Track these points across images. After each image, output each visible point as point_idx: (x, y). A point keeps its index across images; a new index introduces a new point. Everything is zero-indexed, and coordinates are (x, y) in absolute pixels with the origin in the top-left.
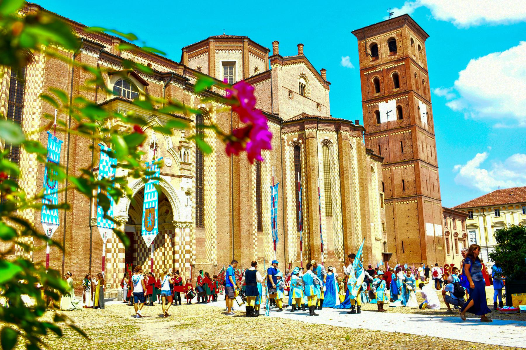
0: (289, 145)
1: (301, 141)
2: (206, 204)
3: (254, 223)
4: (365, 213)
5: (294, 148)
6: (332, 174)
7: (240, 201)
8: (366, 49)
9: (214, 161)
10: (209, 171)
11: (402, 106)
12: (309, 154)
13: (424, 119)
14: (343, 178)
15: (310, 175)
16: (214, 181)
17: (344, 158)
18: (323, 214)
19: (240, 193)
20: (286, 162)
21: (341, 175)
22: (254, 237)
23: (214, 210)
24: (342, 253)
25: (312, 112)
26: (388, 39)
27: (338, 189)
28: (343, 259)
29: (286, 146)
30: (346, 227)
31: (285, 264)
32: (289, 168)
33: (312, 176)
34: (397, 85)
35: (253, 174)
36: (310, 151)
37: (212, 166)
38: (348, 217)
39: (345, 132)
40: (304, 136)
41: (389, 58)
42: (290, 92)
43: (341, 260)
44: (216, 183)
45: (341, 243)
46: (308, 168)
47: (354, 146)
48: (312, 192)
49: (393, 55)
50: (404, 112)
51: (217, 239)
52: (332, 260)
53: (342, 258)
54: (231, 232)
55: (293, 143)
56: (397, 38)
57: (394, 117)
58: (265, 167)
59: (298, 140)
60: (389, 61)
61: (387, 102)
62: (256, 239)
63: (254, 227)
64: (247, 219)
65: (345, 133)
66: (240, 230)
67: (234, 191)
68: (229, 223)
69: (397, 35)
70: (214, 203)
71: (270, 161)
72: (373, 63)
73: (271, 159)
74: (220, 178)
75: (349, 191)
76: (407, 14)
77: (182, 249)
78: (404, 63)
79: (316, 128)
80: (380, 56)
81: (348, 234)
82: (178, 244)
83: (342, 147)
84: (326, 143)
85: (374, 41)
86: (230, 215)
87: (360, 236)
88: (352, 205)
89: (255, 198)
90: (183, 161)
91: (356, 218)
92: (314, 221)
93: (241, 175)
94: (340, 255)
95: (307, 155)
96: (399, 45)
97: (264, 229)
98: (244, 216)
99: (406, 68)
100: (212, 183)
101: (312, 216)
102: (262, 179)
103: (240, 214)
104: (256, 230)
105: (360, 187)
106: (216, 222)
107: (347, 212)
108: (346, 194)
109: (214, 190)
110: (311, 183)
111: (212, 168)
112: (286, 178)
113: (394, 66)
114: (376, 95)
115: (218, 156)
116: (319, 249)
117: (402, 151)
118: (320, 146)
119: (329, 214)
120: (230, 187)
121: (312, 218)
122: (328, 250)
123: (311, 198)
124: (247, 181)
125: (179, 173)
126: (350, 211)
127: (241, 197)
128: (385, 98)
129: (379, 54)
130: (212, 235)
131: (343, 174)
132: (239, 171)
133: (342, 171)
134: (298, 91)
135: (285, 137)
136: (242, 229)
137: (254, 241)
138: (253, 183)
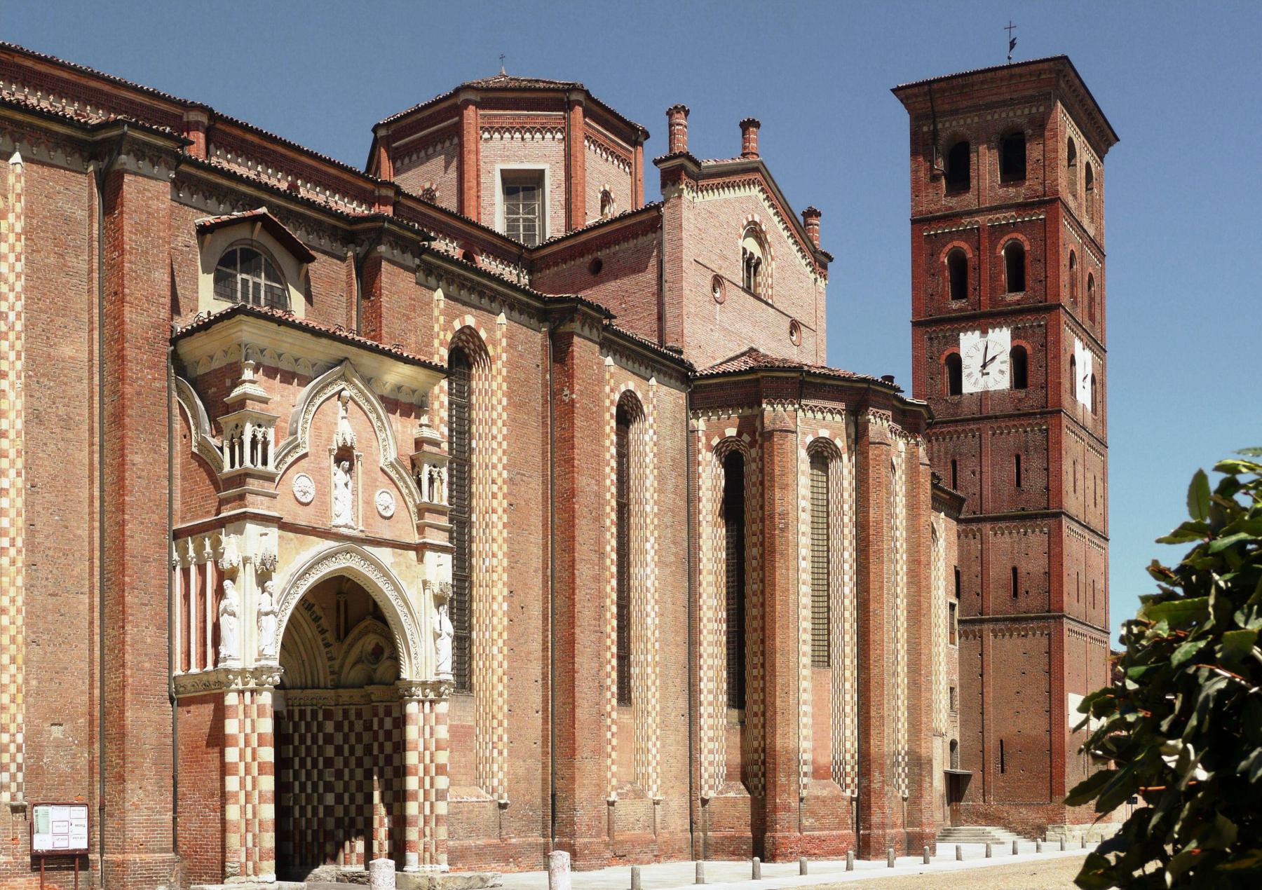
0: (709, 448)
2: (476, 627)
3: (609, 681)
4: (920, 659)
5: (726, 457)
6: (835, 542)
7: (574, 617)
9: (500, 495)
10: (487, 525)
12: (772, 480)
14: (867, 558)
15: (773, 544)
16: (500, 555)
17: (873, 497)
18: (806, 660)
19: (574, 594)
22: (609, 721)
23: (500, 643)
24: (853, 774)
25: (778, 348)
27: (849, 589)
29: (704, 451)
30: (869, 701)
31: (691, 801)
33: (779, 548)
35: (608, 535)
36: (777, 472)
37: (494, 511)
38: (874, 671)
39: (878, 420)
40: (758, 423)
43: (848, 792)
44: (505, 562)
45: (851, 744)
46: (767, 522)
47: (899, 461)
48: (778, 593)
51: (509, 731)
52: (825, 793)
53: (852, 786)
54: (545, 710)
58: (644, 514)
59: (739, 434)
62: (614, 728)
63: (609, 695)
64: (593, 672)
65: (879, 424)
66: (573, 703)
67: (557, 586)
68: (540, 682)
70: (500, 621)
71: (656, 495)
73: (660, 491)
74: (516, 547)
75: (881, 595)
81: (873, 721)
83: (868, 465)
84: (821, 455)
86: (545, 658)
87: (903, 725)
88: (889, 638)
89: (614, 609)
90: (426, 499)
91: (895, 674)
92: (779, 681)
93: (579, 539)
94: (848, 780)
95: (767, 484)
97: (634, 700)
98: (584, 663)
100: (495, 561)
101: (774, 666)
102: (633, 551)
103: (573, 657)
104: (614, 702)
105: (908, 583)
106: (505, 679)
107: (872, 658)
108: (873, 606)
109: (500, 585)
110: (774, 567)
111: (495, 517)
115: (511, 479)
116: (789, 760)
118: (803, 454)
119: (823, 658)
120: (545, 575)
121: (774, 670)
122: (814, 762)
123: (774, 612)
124: (594, 557)
125: (415, 539)
126: (881, 656)
127: (578, 607)
130: (493, 717)
131: (868, 546)
132: (573, 526)
133: (864, 534)
135: (701, 424)
136: (579, 702)
137: (609, 735)
138: (608, 562)
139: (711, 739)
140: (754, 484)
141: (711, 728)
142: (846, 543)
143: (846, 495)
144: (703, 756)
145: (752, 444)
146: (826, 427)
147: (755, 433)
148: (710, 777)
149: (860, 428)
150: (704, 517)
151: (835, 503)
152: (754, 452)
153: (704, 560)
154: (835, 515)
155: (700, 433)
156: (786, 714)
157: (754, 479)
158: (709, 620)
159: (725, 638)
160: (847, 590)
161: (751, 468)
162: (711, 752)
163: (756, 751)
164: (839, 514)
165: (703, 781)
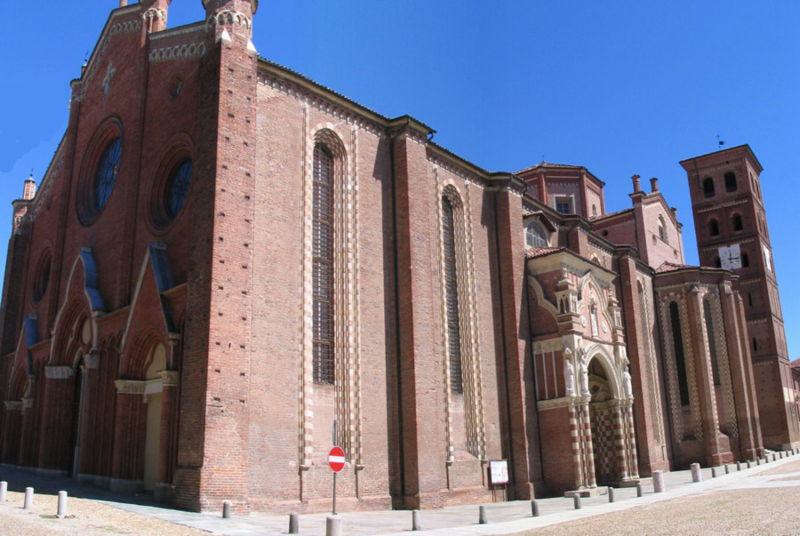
11: (748, 252)
13: (769, 267)
34: (739, 227)
41: (728, 194)
42: (654, 237)
50: (750, 258)
57: (738, 265)
61: (729, 246)
72: (708, 200)
76: (747, 145)
96: (738, 180)
99: (750, 207)
114: (714, 238)
117: (751, 304)
128: (728, 242)
134: (658, 234)
145: (682, 298)
152: (682, 301)
161: (682, 308)
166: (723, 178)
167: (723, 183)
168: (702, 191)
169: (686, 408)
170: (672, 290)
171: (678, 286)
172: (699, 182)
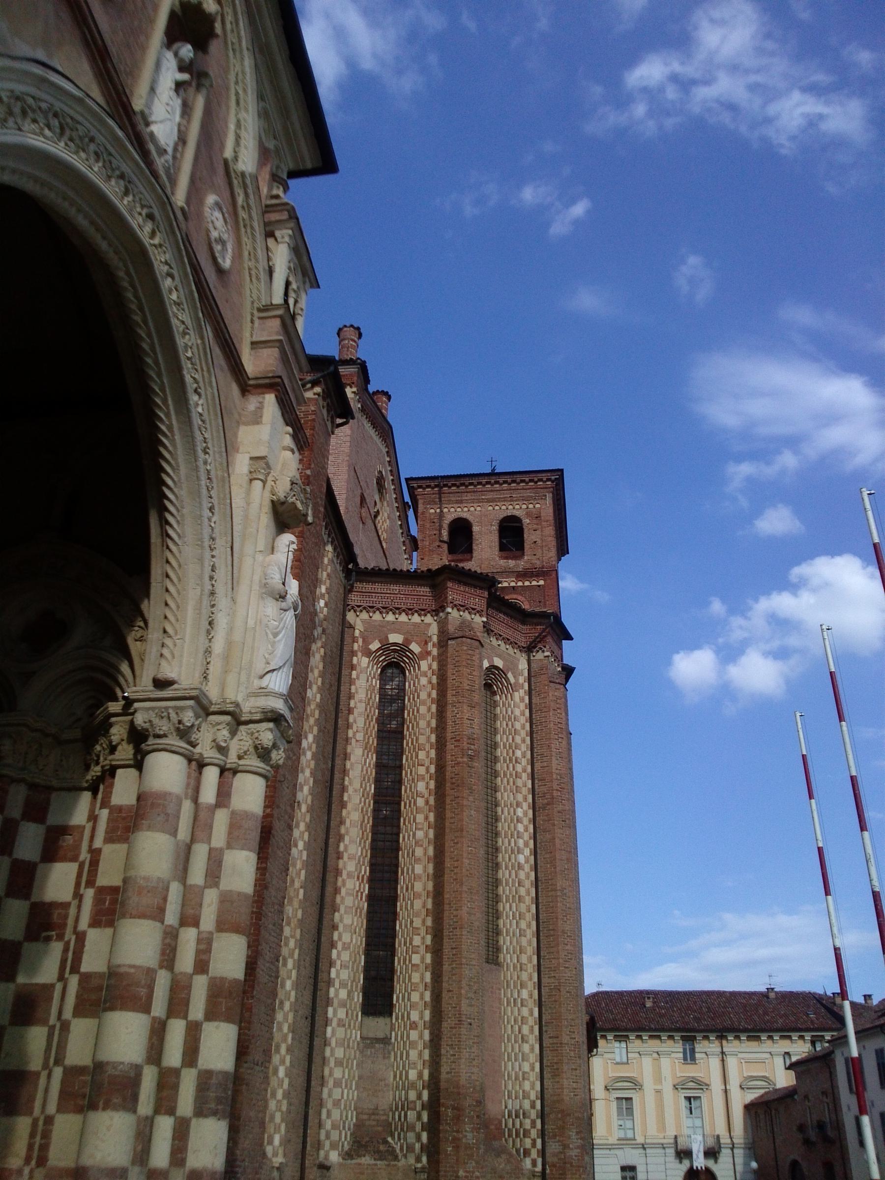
0: (368, 653)
1: (415, 648)
6: (504, 796)
8: (440, 530)
20: (350, 711)
21: (540, 802)
24: (534, 1133)
26: (502, 516)
28: (539, 1161)
29: (360, 654)
32: (360, 736)
45: (532, 1087)
49: (512, 559)
55: (386, 647)
56: (528, 521)
59: (407, 642)
60: (499, 570)
69: (529, 514)
77: (186, 961)
78: (542, 582)
79: (484, 613)
80: (475, 554)
82: (159, 914)
85: (465, 515)
112: (345, 772)
113: (513, 584)
129: (474, 547)
139: (339, 1063)
140: (423, 703)
141: (340, 1043)
142: (520, 797)
143: (518, 739)
144: (325, 1091)
146: (499, 656)
147: (426, 643)
148: (334, 1127)
149: (533, 665)
150: (354, 734)
151: (505, 747)
153: (351, 790)
154: (505, 761)
155: (357, 633)
156: (474, 1026)
157: (423, 695)
158: (350, 875)
159: (366, 904)
160: (521, 858)
162: (337, 1084)
163: (413, 1086)
164: (511, 760)
165: (323, 1134)
166: (495, 527)
167: (495, 538)
168: (445, 546)
169: (378, 1026)
170: (396, 627)
171: (416, 618)
172: (441, 527)
